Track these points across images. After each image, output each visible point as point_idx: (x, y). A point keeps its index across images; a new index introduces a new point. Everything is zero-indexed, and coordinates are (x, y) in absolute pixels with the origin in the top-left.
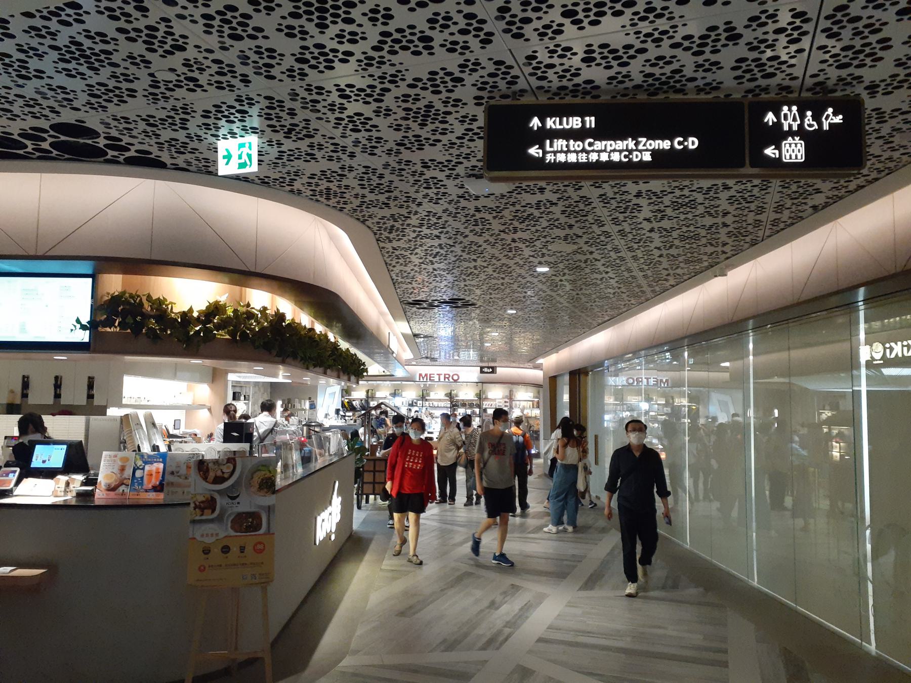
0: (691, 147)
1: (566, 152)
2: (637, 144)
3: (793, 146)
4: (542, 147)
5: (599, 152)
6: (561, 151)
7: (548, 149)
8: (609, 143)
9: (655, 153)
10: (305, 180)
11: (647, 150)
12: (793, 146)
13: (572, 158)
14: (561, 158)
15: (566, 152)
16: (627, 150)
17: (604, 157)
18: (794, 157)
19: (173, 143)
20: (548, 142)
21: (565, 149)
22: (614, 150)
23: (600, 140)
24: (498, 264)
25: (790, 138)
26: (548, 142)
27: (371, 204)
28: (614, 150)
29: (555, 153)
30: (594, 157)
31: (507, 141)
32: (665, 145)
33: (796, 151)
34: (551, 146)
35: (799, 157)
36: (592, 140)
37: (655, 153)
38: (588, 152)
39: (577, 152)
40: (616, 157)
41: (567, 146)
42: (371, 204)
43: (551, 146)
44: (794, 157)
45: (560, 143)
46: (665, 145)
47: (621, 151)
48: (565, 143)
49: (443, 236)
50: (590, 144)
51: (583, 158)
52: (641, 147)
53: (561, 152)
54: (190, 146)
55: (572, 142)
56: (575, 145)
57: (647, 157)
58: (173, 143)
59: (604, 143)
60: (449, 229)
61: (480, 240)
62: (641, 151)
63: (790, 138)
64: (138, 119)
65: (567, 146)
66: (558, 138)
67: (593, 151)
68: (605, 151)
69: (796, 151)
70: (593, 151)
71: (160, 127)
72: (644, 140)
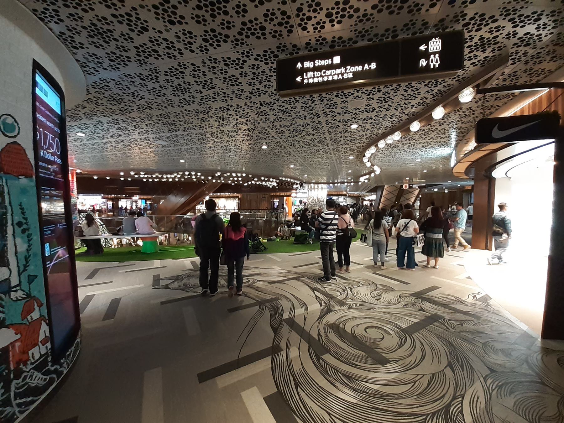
0: (372, 68)
1: (313, 78)
2: (346, 70)
3: (435, 43)
4: (302, 77)
5: (328, 76)
6: (311, 78)
7: (305, 77)
8: (333, 71)
9: (354, 73)
10: (213, 111)
11: (350, 72)
12: (435, 43)
13: (316, 80)
14: (311, 81)
15: (313, 78)
16: (341, 73)
17: (330, 78)
18: (435, 49)
19: (155, 90)
20: (305, 74)
21: (313, 76)
22: (335, 74)
23: (329, 70)
24: (287, 151)
25: (434, 39)
26: (305, 74)
27: (241, 123)
28: (335, 74)
29: (308, 79)
30: (325, 79)
31: (287, 78)
32: (360, 68)
33: (436, 46)
34: (306, 75)
35: (438, 48)
36: (324, 71)
37: (354, 73)
38: (323, 77)
39: (318, 77)
40: (336, 78)
41: (314, 75)
42: (241, 123)
43: (306, 75)
44: (435, 49)
45: (310, 74)
46: (360, 68)
47: (338, 75)
48: (312, 73)
49: (267, 138)
50: (324, 73)
51: (321, 80)
52: (348, 71)
53: (311, 78)
54: (162, 92)
55: (315, 73)
56: (317, 74)
57: (351, 76)
58: (155, 90)
59: (330, 71)
60: (269, 135)
61: (281, 140)
62: (348, 73)
63: (434, 39)
64: (135, 76)
65: (314, 75)
66: (309, 72)
67: (325, 76)
68: (331, 75)
69: (436, 46)
70: (325, 76)
71: (147, 80)
72: (349, 67)
